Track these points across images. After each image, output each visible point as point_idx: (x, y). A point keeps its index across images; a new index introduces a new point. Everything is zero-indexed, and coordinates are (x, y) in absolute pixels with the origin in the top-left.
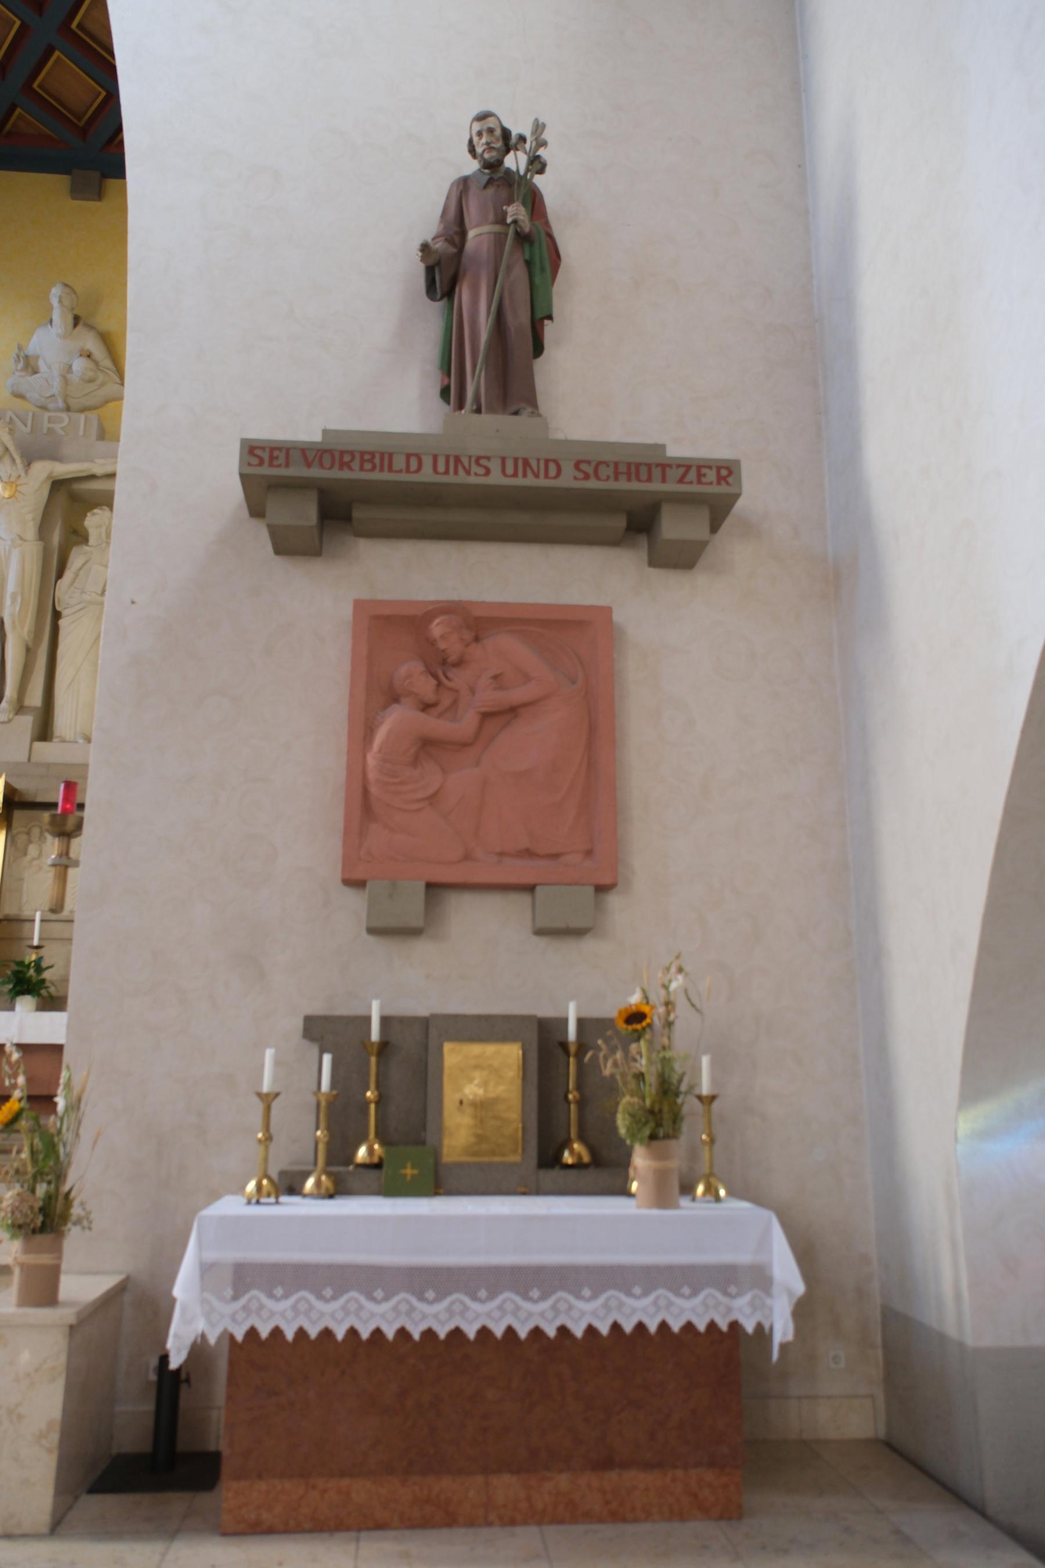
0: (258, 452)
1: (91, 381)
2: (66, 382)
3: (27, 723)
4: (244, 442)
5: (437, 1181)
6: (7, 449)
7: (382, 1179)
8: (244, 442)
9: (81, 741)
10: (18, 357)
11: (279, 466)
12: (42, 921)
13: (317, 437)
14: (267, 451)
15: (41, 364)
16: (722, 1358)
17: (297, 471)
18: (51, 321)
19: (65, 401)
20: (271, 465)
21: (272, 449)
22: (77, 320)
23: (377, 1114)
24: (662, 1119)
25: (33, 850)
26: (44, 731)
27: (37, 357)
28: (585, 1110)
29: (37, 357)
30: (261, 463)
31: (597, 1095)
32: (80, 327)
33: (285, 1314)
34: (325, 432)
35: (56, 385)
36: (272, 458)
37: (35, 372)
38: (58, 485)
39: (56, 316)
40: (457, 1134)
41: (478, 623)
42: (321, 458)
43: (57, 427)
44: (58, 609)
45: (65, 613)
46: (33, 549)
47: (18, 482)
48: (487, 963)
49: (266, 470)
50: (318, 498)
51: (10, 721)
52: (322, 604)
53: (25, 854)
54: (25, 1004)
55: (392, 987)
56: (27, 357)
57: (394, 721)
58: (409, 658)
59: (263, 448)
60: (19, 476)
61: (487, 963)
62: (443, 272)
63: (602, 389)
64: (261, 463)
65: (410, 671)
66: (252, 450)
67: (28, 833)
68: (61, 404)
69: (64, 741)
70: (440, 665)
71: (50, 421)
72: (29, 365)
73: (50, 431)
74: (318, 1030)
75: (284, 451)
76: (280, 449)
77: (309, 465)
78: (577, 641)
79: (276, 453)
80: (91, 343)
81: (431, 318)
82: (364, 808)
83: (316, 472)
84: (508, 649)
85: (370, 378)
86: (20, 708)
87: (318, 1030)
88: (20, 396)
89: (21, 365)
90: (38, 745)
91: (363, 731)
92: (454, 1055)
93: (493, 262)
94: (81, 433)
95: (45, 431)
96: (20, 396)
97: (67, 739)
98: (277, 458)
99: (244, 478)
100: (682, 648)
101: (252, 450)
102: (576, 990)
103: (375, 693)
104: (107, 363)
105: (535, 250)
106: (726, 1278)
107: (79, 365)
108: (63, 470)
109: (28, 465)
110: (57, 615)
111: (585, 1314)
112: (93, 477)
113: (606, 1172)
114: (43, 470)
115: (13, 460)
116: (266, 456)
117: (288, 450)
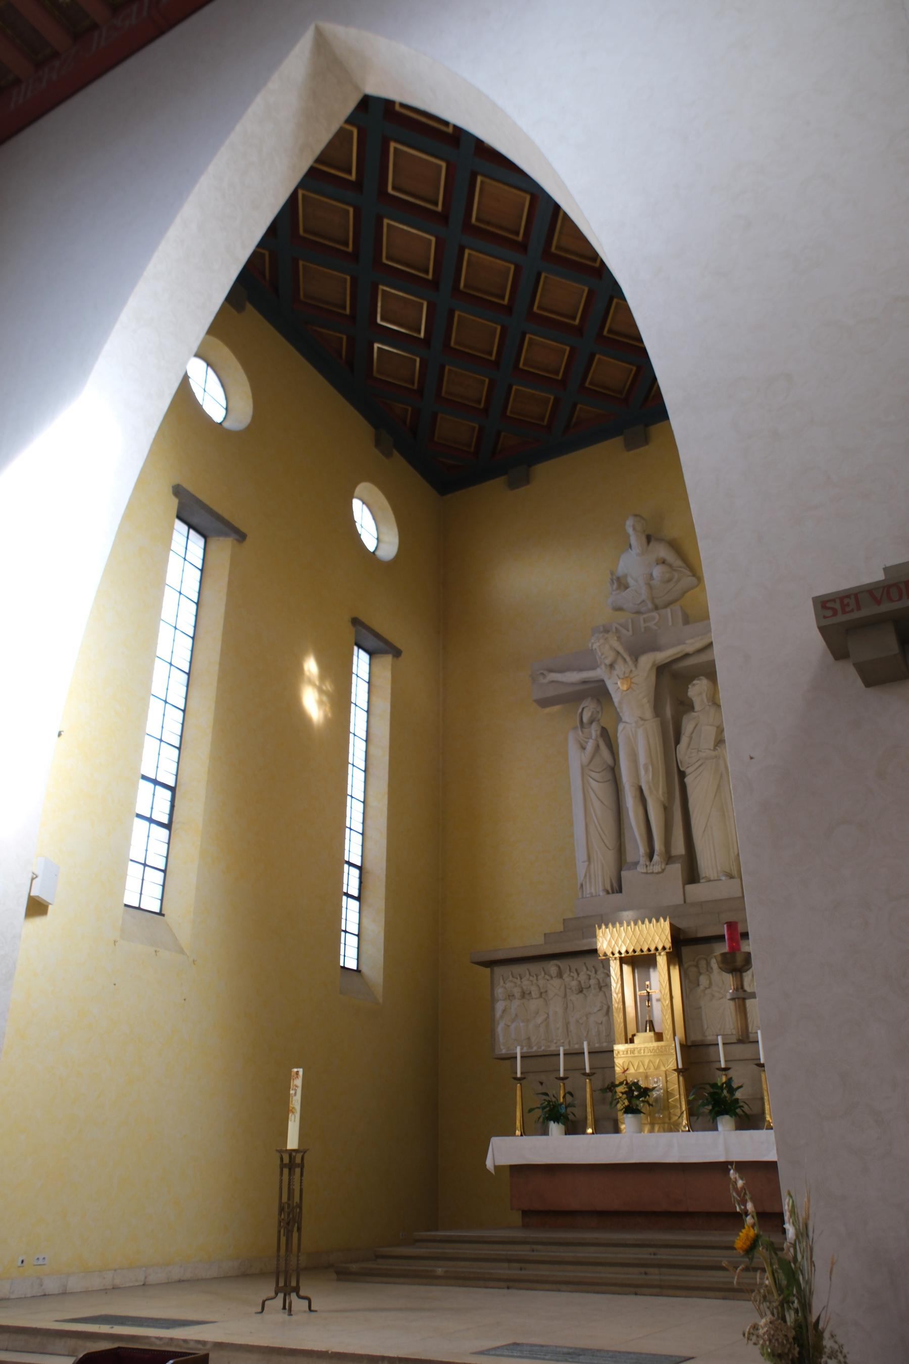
0: (829, 605)
1: (669, 581)
2: (650, 587)
3: (676, 869)
4: (815, 600)
6: (618, 653)
8: (815, 600)
9: (723, 878)
10: (612, 580)
11: (852, 611)
12: (724, 1044)
13: (880, 576)
14: (838, 601)
15: (631, 581)
17: (869, 610)
18: (630, 546)
19: (653, 602)
20: (844, 612)
21: (842, 599)
22: (649, 539)
25: (703, 980)
26: (692, 875)
27: (626, 576)
29: (626, 576)
30: (835, 613)
32: (652, 544)
34: (886, 570)
35: (644, 591)
36: (844, 606)
37: (626, 587)
38: (661, 670)
39: (633, 540)
42: (888, 593)
43: (651, 624)
44: (682, 769)
45: (688, 771)
46: (652, 725)
47: (632, 675)
49: (841, 618)
51: (663, 870)
53: (698, 985)
54: (725, 1123)
56: (618, 579)
59: (834, 600)
60: (631, 671)
64: (835, 613)
66: (823, 604)
67: (697, 966)
68: (650, 606)
69: (710, 881)
71: (645, 621)
72: (621, 583)
73: (647, 629)
75: (853, 597)
76: (848, 596)
77: (879, 602)
79: (846, 601)
80: (663, 551)
83: (886, 607)
86: (669, 859)
88: (619, 609)
89: (615, 586)
90: (689, 887)
94: (670, 624)
95: (643, 630)
96: (619, 609)
97: (712, 878)
98: (848, 605)
99: (822, 629)
101: (823, 604)
104: (678, 563)
107: (657, 571)
108: (662, 657)
109: (636, 660)
110: (682, 775)
112: (687, 656)
114: (647, 661)
115: (625, 660)
116: (837, 606)
117: (856, 595)
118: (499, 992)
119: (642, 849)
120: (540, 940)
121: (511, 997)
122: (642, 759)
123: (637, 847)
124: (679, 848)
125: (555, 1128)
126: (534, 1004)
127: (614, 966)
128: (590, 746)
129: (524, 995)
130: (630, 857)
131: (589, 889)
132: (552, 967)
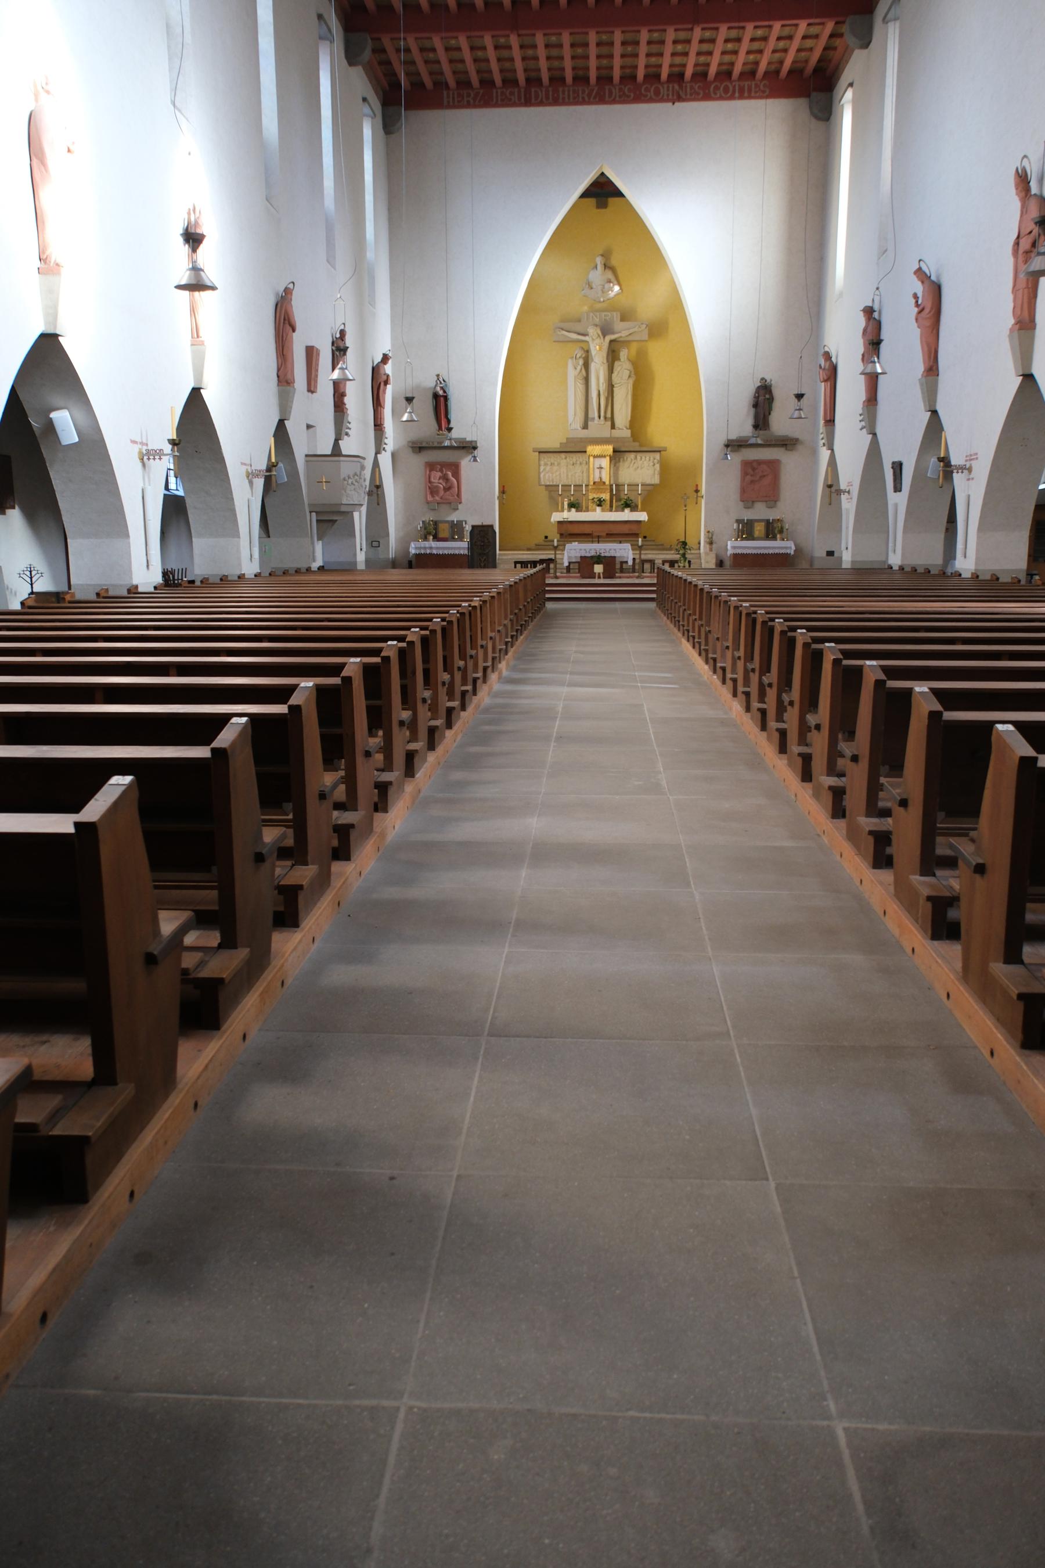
3: (609, 423)
5: (753, 539)
7: (746, 539)
16: (786, 556)
23: (746, 530)
24: (781, 531)
26: (613, 427)
28: (772, 530)
31: (774, 529)
33: (739, 551)
38: (611, 341)
39: (599, 267)
40: (756, 534)
41: (760, 462)
46: (606, 366)
48: (760, 512)
50: (734, 445)
52: (735, 459)
54: (627, 510)
55: (747, 515)
57: (748, 478)
58: (750, 468)
61: (760, 512)
62: (755, 406)
63: (781, 422)
65: (750, 471)
70: (754, 469)
74: (738, 521)
78: (774, 466)
81: (753, 410)
82: (743, 491)
84: (764, 467)
85: (743, 426)
86: (605, 418)
87: (738, 521)
91: (743, 479)
92: (756, 524)
93: (763, 399)
100: (790, 463)
102: (772, 515)
103: (745, 474)
105: (771, 400)
106: (786, 548)
108: (613, 337)
110: (613, 386)
111: (771, 551)
113: (774, 538)
114: (608, 338)
118: (542, 463)
119: (596, 415)
120: (558, 446)
121: (546, 464)
122: (602, 380)
123: (594, 412)
124: (609, 415)
125: (573, 510)
126: (555, 468)
127: (591, 459)
128: (579, 368)
129: (552, 464)
130: (590, 416)
131: (573, 426)
132: (563, 455)
